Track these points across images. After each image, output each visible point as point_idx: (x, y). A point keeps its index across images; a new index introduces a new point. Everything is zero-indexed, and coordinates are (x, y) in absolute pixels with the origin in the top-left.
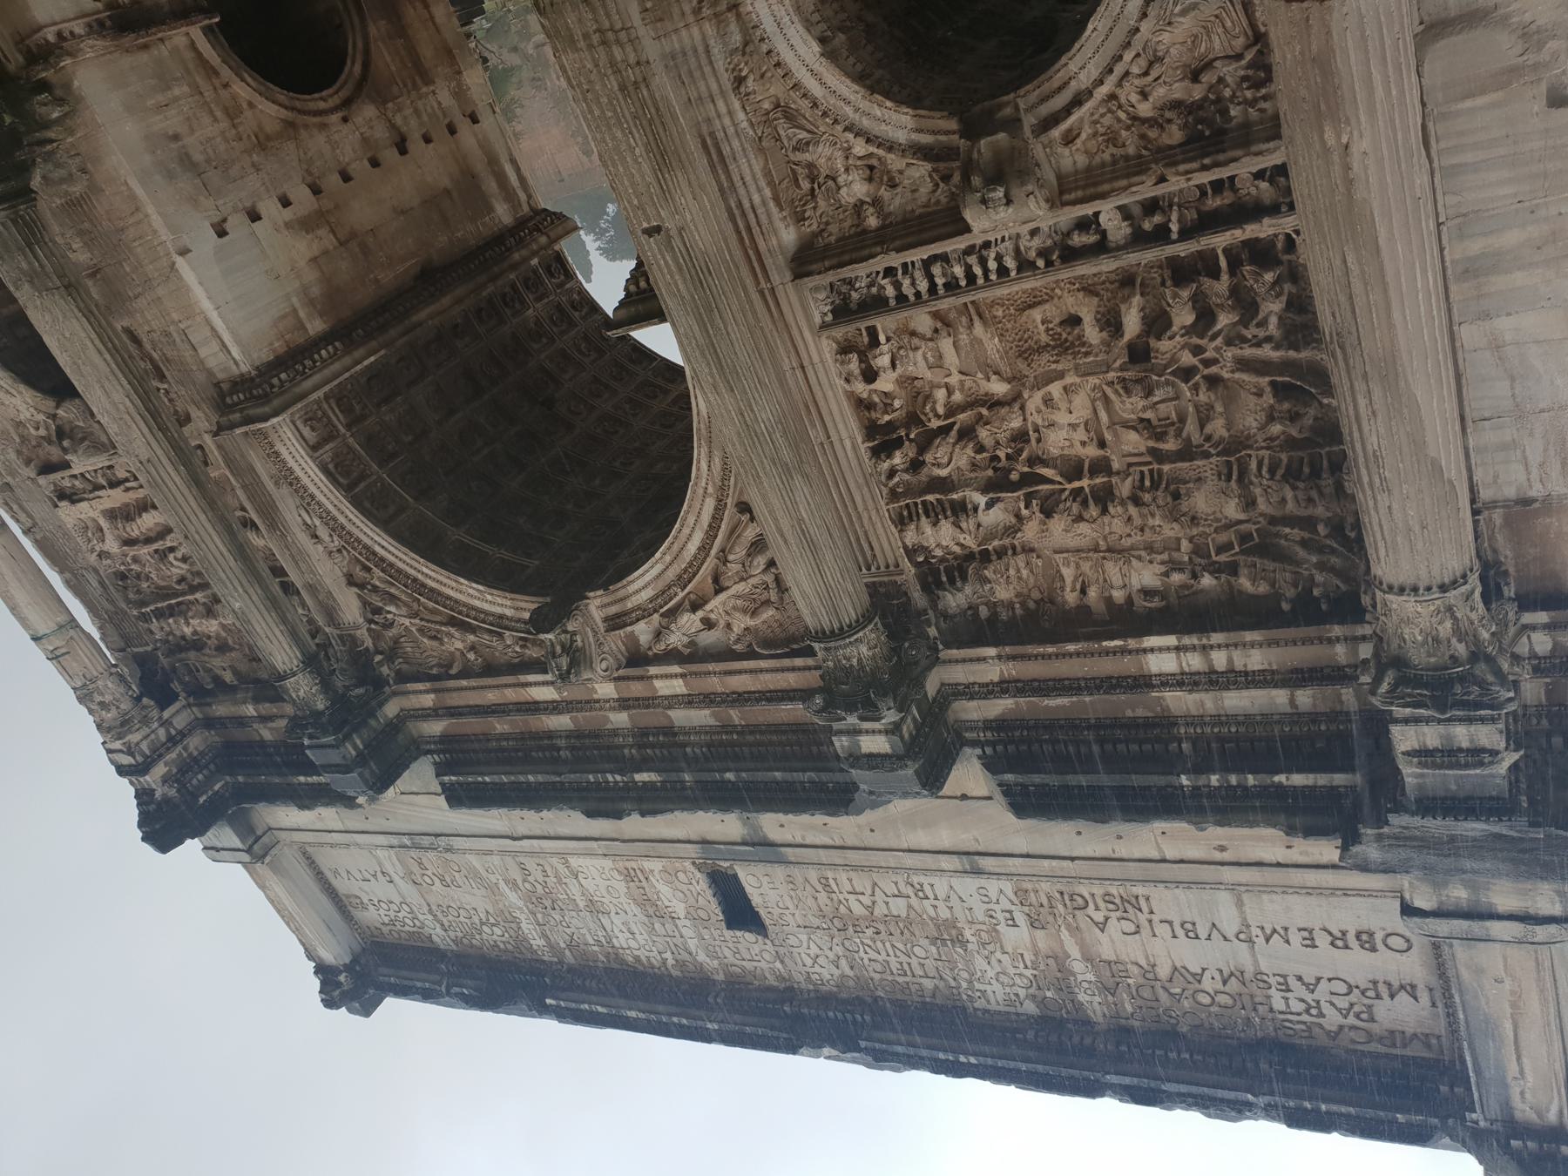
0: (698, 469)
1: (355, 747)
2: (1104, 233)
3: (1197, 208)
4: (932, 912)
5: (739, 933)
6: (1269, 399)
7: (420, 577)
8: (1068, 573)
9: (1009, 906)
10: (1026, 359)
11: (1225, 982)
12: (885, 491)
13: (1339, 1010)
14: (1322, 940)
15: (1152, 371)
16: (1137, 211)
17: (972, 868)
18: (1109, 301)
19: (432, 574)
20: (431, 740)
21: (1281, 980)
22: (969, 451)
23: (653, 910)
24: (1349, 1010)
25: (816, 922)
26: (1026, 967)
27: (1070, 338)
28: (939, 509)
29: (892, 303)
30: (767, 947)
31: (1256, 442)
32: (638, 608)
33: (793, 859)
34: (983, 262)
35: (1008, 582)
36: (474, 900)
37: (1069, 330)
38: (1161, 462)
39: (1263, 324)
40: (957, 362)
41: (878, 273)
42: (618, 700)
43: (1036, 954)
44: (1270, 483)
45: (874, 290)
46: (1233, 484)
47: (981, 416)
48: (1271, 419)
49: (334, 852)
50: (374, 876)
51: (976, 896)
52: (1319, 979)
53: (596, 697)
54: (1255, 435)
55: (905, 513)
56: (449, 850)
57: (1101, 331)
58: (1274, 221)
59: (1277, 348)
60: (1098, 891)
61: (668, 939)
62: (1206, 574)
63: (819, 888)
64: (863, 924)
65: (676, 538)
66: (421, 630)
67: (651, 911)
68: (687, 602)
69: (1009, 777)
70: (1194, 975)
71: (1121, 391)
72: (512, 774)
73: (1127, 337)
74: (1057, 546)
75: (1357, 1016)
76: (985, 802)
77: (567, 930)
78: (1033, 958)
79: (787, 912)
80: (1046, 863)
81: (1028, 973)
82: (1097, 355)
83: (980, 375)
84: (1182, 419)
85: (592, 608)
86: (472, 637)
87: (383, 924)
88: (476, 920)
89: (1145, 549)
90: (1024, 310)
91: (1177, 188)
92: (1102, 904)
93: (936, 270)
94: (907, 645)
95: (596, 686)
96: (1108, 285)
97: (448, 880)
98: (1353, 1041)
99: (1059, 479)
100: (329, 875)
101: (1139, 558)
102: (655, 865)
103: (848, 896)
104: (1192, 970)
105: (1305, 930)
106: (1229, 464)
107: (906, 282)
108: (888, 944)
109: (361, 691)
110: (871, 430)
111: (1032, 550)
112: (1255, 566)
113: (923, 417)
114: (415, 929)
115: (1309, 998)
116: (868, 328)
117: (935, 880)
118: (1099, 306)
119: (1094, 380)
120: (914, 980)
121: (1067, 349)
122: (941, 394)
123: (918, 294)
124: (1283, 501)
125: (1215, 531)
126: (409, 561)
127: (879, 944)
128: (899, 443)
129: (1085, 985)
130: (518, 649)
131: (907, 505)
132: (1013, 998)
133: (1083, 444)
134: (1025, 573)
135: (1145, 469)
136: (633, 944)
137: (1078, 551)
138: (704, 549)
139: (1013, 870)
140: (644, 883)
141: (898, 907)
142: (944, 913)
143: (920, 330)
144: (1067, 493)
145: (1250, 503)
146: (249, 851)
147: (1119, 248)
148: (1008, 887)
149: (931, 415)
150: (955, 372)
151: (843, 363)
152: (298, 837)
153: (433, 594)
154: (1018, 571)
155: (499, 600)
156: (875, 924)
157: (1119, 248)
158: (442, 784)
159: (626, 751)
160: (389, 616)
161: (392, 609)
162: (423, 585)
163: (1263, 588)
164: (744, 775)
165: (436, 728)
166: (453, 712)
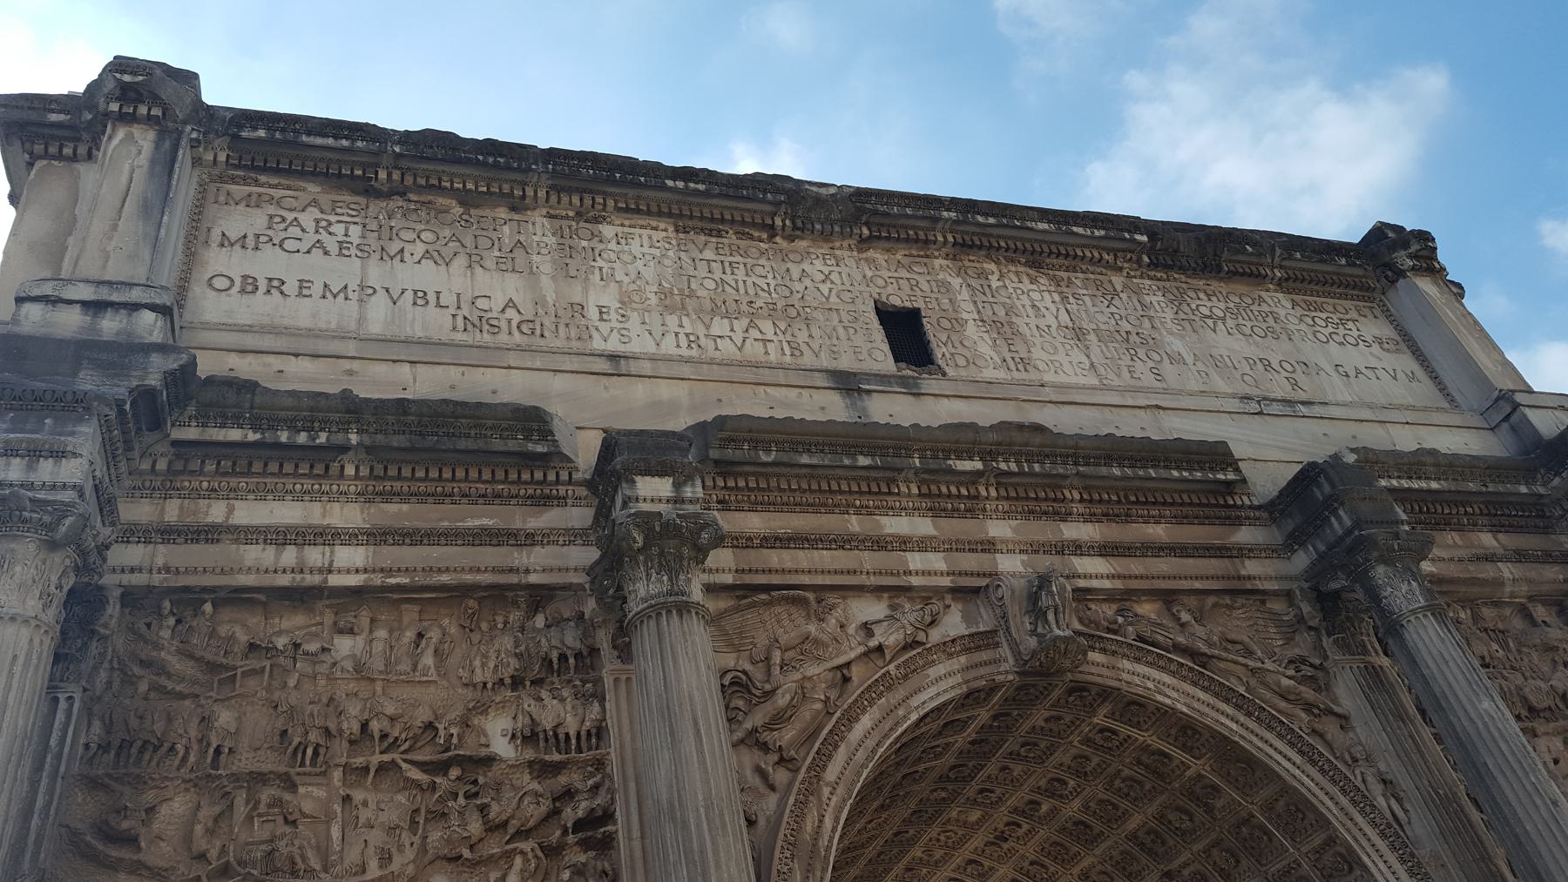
0: (837, 820)
1: (1339, 518)
4: (685, 320)
5: (908, 304)
7: (1242, 719)
8: (428, 660)
9: (601, 325)
11: (402, 251)
12: (608, 769)
13: (299, 225)
14: (291, 287)
17: (618, 363)
19: (1223, 720)
20: (1253, 522)
21: (344, 252)
23: (1003, 329)
24: (291, 224)
25: (817, 315)
26: (601, 269)
28: (552, 740)
30: (878, 290)
32: (950, 656)
33: (817, 374)
36: (1228, 343)
42: (995, 551)
43: (587, 279)
47: (471, 847)
49: (1411, 401)
50: (1358, 372)
51: (633, 335)
52: (308, 252)
53: (1024, 557)
56: (1246, 398)
60: (503, 338)
61: (992, 300)
62: (280, 647)
63: (804, 348)
64: (765, 312)
65: (886, 736)
66: (1249, 653)
67: (1006, 328)
68: (888, 657)
69: (540, 449)
70: (432, 257)
71: (298, 860)
72: (1140, 478)
74: (432, 689)
75: (284, 220)
76: (581, 425)
77: (1115, 310)
78: (591, 277)
79: (847, 324)
80: (538, 364)
81: (600, 263)
84: (250, 819)
85: (1011, 661)
86: (1181, 639)
87: (1354, 321)
88: (1230, 323)
92: (504, 325)
94: (611, 592)
95: (1021, 569)
97: (1260, 366)
98: (296, 198)
99: (404, 766)
100: (1420, 373)
102: (989, 374)
103: (774, 338)
104: (430, 263)
105: (305, 296)
106: (215, 764)
108: (742, 291)
109: (1334, 585)
110: (606, 844)
113: (540, 854)
114: (1314, 314)
115: (324, 236)
117: (674, 351)
120: (722, 258)
126: (1255, 739)
127: (751, 291)
128: (579, 825)
129: (544, 251)
130: (1120, 620)
131: (590, 749)
132: (623, 241)
133: (365, 804)
134: (477, 663)
135: (308, 769)
136: (1037, 296)
138: (850, 718)
139: (575, 358)
140: (1008, 356)
141: (720, 326)
142: (672, 321)
144: (402, 748)
145: (206, 721)
146: (1516, 406)
148: (598, 344)
149: (530, 855)
152: (1455, 419)
153: (1226, 694)
154: (483, 665)
155: (1137, 680)
156: (751, 310)
158: (1237, 470)
159: (993, 493)
160: (1291, 672)
161: (1285, 682)
162: (1238, 707)
164: (847, 462)
165: (1245, 535)
166: (1221, 552)
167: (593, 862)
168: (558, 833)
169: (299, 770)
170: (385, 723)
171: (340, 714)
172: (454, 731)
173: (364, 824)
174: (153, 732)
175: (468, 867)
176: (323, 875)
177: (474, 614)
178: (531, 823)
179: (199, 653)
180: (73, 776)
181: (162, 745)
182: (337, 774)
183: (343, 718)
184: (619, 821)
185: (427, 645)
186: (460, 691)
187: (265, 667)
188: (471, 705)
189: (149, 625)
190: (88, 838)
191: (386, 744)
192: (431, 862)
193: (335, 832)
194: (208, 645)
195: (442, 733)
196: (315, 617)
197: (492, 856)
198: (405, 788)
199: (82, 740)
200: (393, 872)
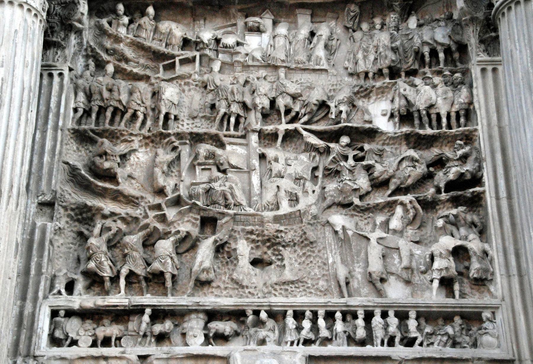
2: (206, 327)
3: (127, 329)
6: (121, 173)
8: (320, 52)
10: (306, 239)
12: (476, 144)
15: (201, 209)
16: (176, 338)
18: (225, 273)
22: (379, 168)
27: (265, 249)
28: (425, 119)
29: (413, 314)
31: (140, 141)
34: (315, 328)
35: (377, 47)
37: (265, 257)
38: (217, 135)
39: (105, 229)
40: (369, 249)
41: (421, 344)
44: (137, 108)
45: (428, 329)
46: (164, 111)
47: (361, 198)
48: (124, 157)
54: (141, 146)
55: (462, 120)
57: (235, 250)
58: (71, 305)
59: (99, 209)
62: (206, 41)
71: (229, 197)
73: (211, 239)
74: (323, 76)
82: (243, 230)
83: (350, 233)
84: (192, 167)
89: (249, 66)
90: (298, 281)
91: (135, 349)
93: (361, 333)
96: (222, 286)
99: (305, 133)
101: (254, 59)
107: (393, 329)
111: (351, 75)
112: (167, 45)
113: (418, 206)
116: (454, 297)
118: (233, 270)
119: (251, 211)
121: (269, 240)
122: (395, 223)
123: (385, 315)
124: (131, 93)
125: (191, 75)
128: (450, 186)
133: (276, 160)
134: (360, 55)
135: (232, 132)
137: (305, 70)
143: (400, 285)
144: (303, 120)
147: (196, 311)
149: (409, 206)
150: (373, 241)
151: (486, 271)
154: (365, 57)
157: (196, 311)
163: (165, 26)
167: (463, 215)
168: (432, 190)
169: (226, 133)
170: (289, 100)
171: (254, 92)
172: (343, 108)
173: (276, 174)
174: (120, 101)
175: (358, 212)
176: (248, 209)
177: (355, 17)
178: (410, 181)
179: (148, 44)
180: (69, 130)
181: (127, 112)
182: (254, 138)
183: (255, 94)
184: (487, 184)
185: (318, 41)
186: (346, 79)
187: (194, 58)
188: (356, 89)
189: (110, 23)
190: (83, 172)
191: (289, 117)
192: (329, 207)
193: (255, 179)
194: (153, 39)
195: (333, 110)
196: (230, 19)
197: (378, 205)
198: (305, 151)
199: (72, 105)
200: (299, 210)
